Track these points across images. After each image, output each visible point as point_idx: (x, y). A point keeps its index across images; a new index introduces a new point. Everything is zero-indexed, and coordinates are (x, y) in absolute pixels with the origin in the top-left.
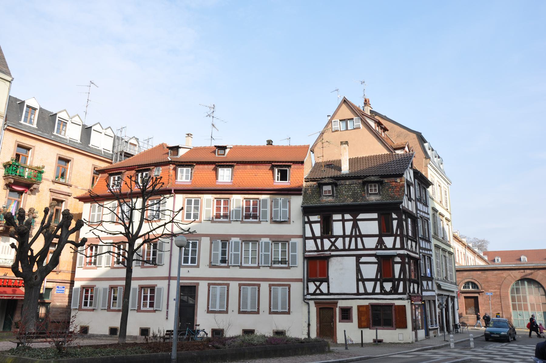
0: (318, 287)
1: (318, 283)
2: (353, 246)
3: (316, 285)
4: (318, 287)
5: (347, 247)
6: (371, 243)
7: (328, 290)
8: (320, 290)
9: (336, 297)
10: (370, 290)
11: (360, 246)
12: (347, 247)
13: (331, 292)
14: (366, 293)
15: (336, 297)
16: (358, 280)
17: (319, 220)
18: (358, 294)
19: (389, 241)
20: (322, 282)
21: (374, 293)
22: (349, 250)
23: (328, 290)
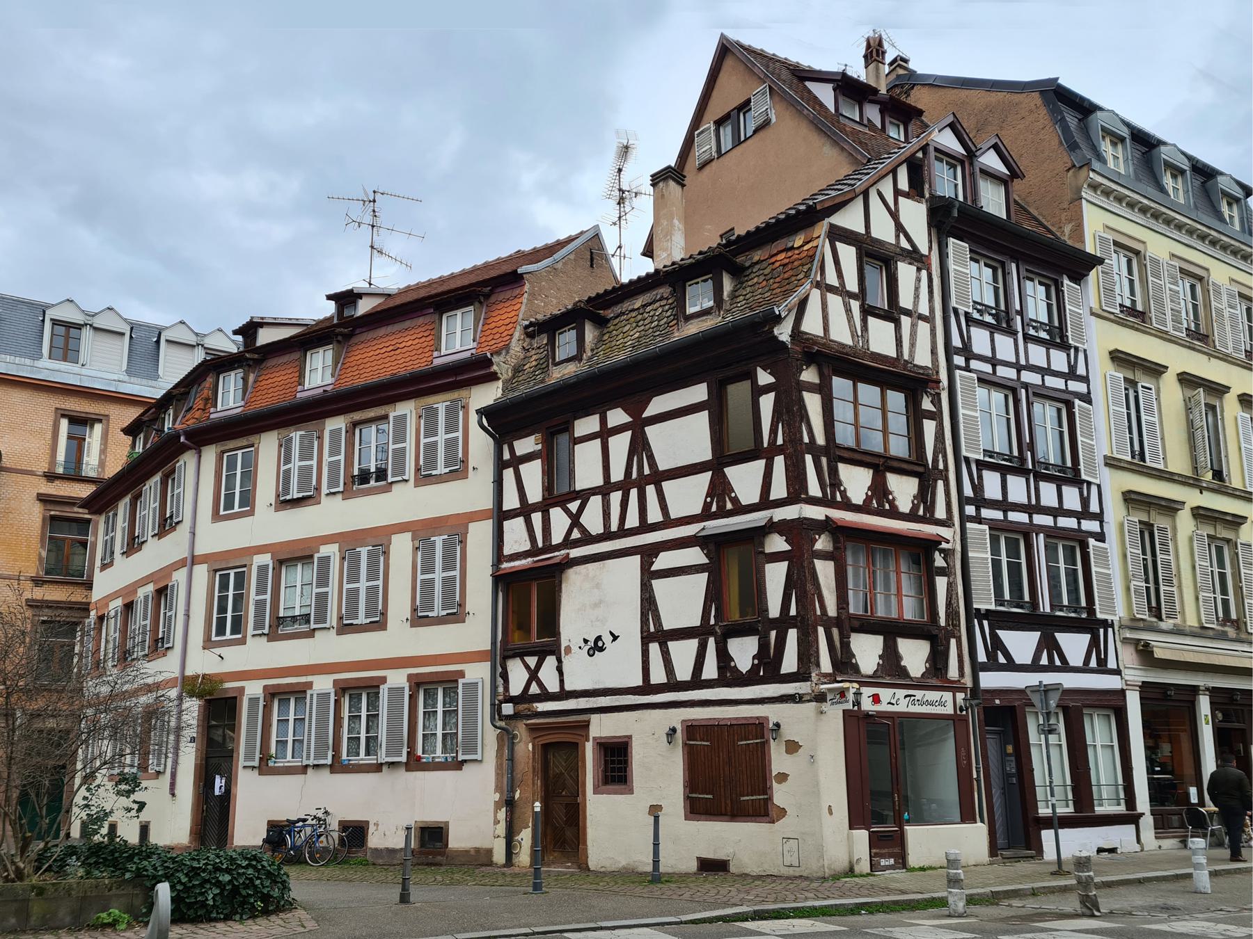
0: (534, 675)
1: (532, 661)
2: (632, 521)
3: (527, 667)
4: (534, 675)
7: (562, 682)
8: (540, 684)
9: (582, 703)
10: (684, 673)
13: (568, 687)
14: (673, 685)
15: (582, 703)
16: (646, 639)
20: (542, 654)
22: (623, 533)
23: (562, 682)
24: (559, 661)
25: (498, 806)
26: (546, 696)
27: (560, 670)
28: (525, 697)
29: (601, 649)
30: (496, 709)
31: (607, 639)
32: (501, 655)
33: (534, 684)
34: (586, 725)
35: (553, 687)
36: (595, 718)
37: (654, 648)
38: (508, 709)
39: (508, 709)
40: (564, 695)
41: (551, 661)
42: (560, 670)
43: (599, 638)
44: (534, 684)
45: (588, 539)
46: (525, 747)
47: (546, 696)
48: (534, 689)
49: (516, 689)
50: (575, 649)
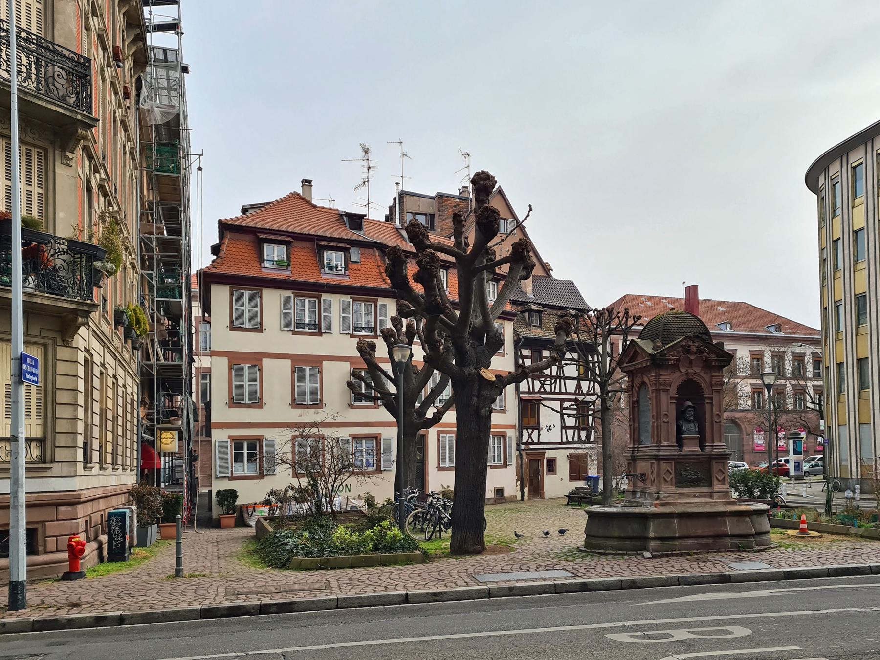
1: (530, 431)
3: (528, 433)
5: (553, 391)
6: (571, 386)
11: (563, 390)
12: (553, 391)
13: (541, 441)
14: (568, 443)
16: (562, 428)
17: (530, 355)
18: (562, 443)
19: (585, 385)
20: (533, 429)
21: (573, 443)
24: (539, 432)
25: (517, 481)
26: (533, 443)
27: (539, 435)
28: (526, 444)
29: (551, 430)
30: (518, 445)
31: (552, 426)
32: (521, 428)
33: (530, 439)
34: (544, 454)
35: (536, 440)
36: (547, 451)
37: (564, 431)
38: (523, 447)
39: (523, 447)
40: (539, 443)
41: (536, 432)
42: (539, 435)
43: (550, 426)
44: (530, 439)
45: (545, 392)
46: (525, 460)
47: (533, 443)
48: (530, 441)
49: (524, 440)
50: (544, 429)
